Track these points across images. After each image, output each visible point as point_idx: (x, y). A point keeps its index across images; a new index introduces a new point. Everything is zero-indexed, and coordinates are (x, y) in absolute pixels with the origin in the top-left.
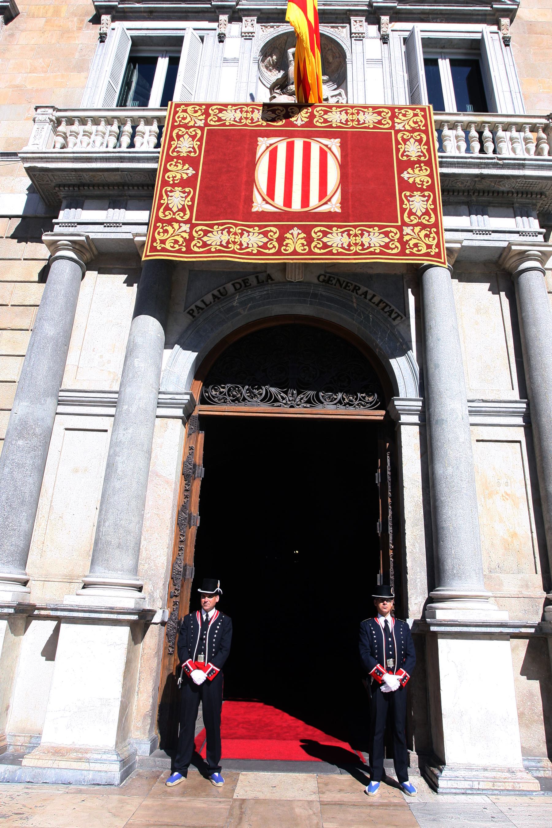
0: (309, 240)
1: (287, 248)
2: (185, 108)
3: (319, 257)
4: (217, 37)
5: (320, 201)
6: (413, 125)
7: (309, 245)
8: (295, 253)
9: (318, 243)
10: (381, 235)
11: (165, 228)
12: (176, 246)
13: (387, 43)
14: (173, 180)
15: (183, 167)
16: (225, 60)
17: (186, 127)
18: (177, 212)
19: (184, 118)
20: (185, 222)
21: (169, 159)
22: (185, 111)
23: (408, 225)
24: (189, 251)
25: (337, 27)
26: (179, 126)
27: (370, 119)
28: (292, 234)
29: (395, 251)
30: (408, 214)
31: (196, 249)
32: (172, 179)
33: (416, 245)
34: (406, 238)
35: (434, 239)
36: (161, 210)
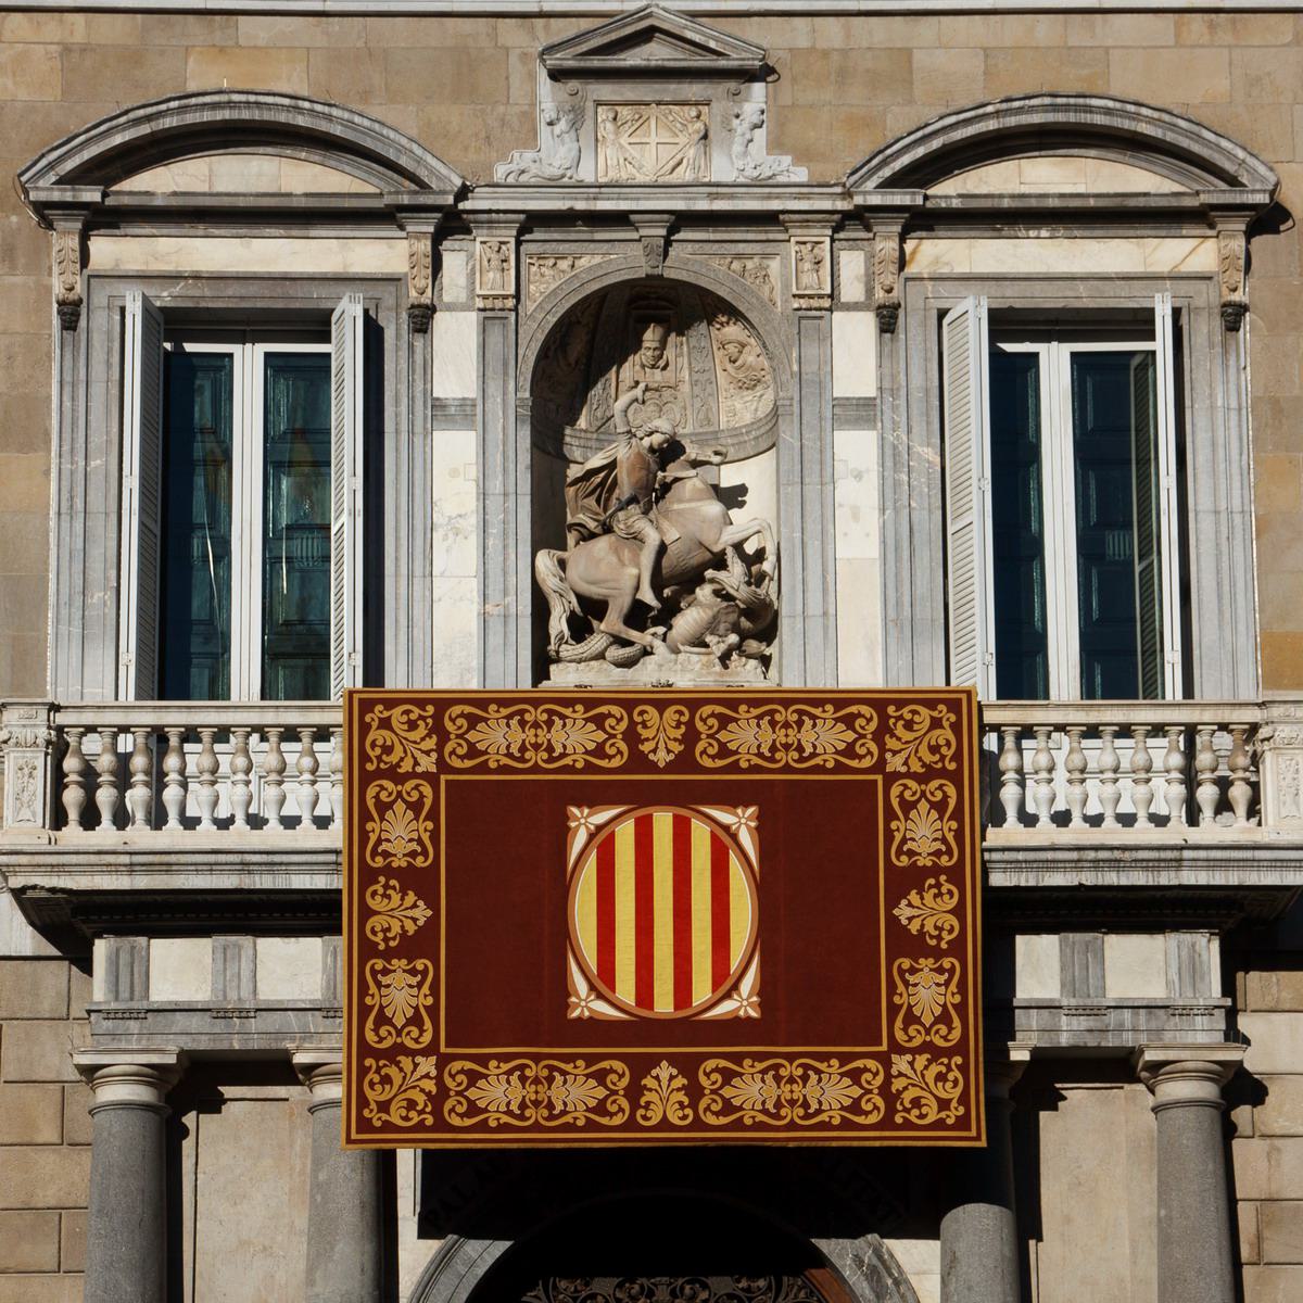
0: (694, 1092)
1: (649, 1114)
2: (386, 714)
3: (716, 1128)
4: (404, 316)
5: (714, 991)
6: (929, 758)
7: (694, 1105)
8: (665, 1125)
9: (714, 1101)
10: (845, 1079)
11: (383, 1072)
12: (413, 1114)
13: (892, 332)
14: (386, 940)
15: (402, 899)
16: (439, 410)
17: (393, 774)
18: (404, 1027)
19: (388, 750)
20: (425, 1052)
21: (368, 876)
22: (385, 724)
23: (901, 1051)
24: (441, 1125)
25: (751, 256)
26: (379, 774)
27: (825, 738)
28: (657, 1078)
29: (873, 1119)
30: (903, 1022)
31: (456, 1121)
32: (381, 935)
33: (916, 1102)
34: (897, 1084)
35: (956, 1082)
36: (370, 1024)
